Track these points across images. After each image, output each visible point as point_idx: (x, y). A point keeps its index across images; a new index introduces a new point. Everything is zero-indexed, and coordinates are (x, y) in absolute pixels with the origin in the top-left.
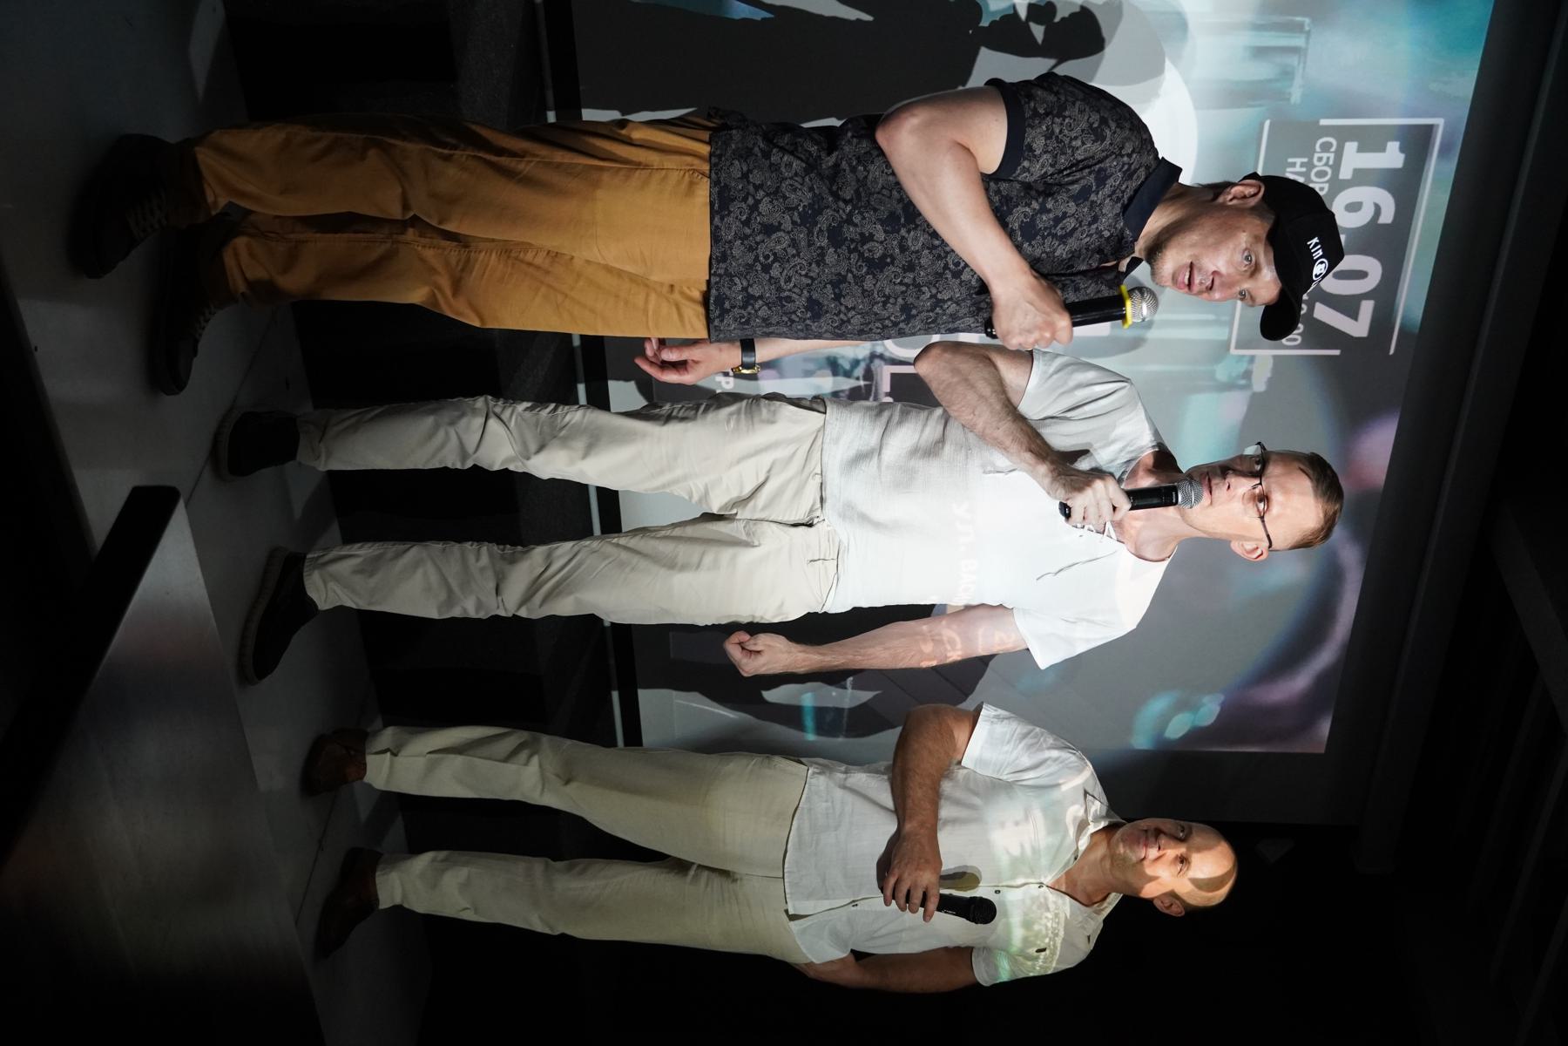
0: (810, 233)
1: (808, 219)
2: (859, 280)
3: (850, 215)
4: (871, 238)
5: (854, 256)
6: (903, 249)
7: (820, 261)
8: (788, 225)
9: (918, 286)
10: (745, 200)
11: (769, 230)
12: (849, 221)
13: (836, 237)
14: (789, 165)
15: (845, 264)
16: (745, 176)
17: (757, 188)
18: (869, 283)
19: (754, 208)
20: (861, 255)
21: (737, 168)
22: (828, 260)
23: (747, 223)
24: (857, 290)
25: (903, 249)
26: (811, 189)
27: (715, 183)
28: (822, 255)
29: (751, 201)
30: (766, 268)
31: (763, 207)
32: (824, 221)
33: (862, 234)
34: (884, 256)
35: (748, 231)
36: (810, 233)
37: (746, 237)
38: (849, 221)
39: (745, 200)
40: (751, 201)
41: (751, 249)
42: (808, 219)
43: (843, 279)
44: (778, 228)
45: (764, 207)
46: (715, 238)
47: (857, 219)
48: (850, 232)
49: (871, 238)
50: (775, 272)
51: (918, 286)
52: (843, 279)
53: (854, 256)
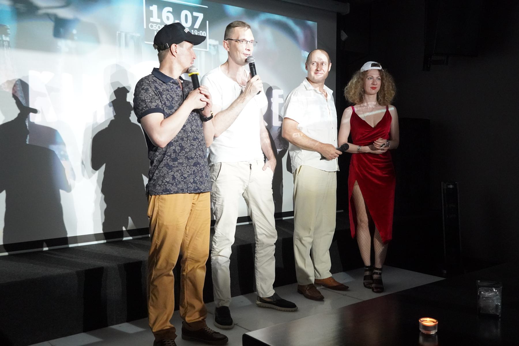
0: (174, 167)
1: (170, 168)
2: (186, 153)
3: (168, 156)
4: (174, 150)
5: (180, 154)
7: (182, 164)
10: (166, 185)
11: (174, 178)
12: (170, 156)
13: (175, 160)
14: (157, 174)
15: (182, 157)
16: (160, 186)
17: (163, 182)
18: (187, 150)
19: (168, 182)
20: (180, 152)
21: (158, 188)
22: (181, 162)
23: (172, 184)
24: (189, 153)
27: (162, 193)
28: (180, 163)
29: (166, 184)
31: (168, 180)
32: (171, 163)
33: (174, 152)
34: (179, 146)
35: (175, 184)
36: (174, 167)
37: (176, 184)
38: (170, 156)
39: (166, 185)
40: (166, 184)
41: (180, 183)
42: (170, 168)
43: (187, 157)
44: (173, 176)
45: (168, 180)
46: (177, 192)
47: (169, 154)
48: (173, 156)
49: (174, 150)
51: (188, 136)
53: (180, 154)
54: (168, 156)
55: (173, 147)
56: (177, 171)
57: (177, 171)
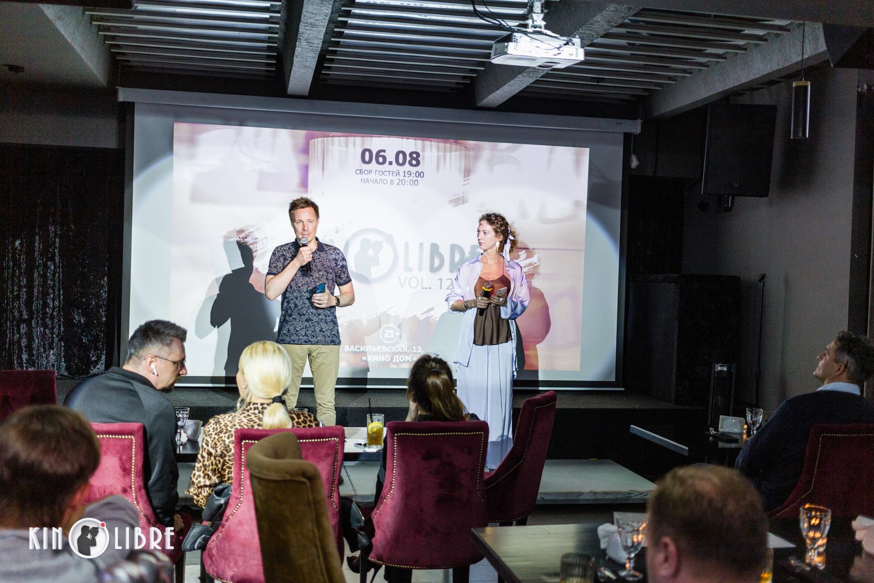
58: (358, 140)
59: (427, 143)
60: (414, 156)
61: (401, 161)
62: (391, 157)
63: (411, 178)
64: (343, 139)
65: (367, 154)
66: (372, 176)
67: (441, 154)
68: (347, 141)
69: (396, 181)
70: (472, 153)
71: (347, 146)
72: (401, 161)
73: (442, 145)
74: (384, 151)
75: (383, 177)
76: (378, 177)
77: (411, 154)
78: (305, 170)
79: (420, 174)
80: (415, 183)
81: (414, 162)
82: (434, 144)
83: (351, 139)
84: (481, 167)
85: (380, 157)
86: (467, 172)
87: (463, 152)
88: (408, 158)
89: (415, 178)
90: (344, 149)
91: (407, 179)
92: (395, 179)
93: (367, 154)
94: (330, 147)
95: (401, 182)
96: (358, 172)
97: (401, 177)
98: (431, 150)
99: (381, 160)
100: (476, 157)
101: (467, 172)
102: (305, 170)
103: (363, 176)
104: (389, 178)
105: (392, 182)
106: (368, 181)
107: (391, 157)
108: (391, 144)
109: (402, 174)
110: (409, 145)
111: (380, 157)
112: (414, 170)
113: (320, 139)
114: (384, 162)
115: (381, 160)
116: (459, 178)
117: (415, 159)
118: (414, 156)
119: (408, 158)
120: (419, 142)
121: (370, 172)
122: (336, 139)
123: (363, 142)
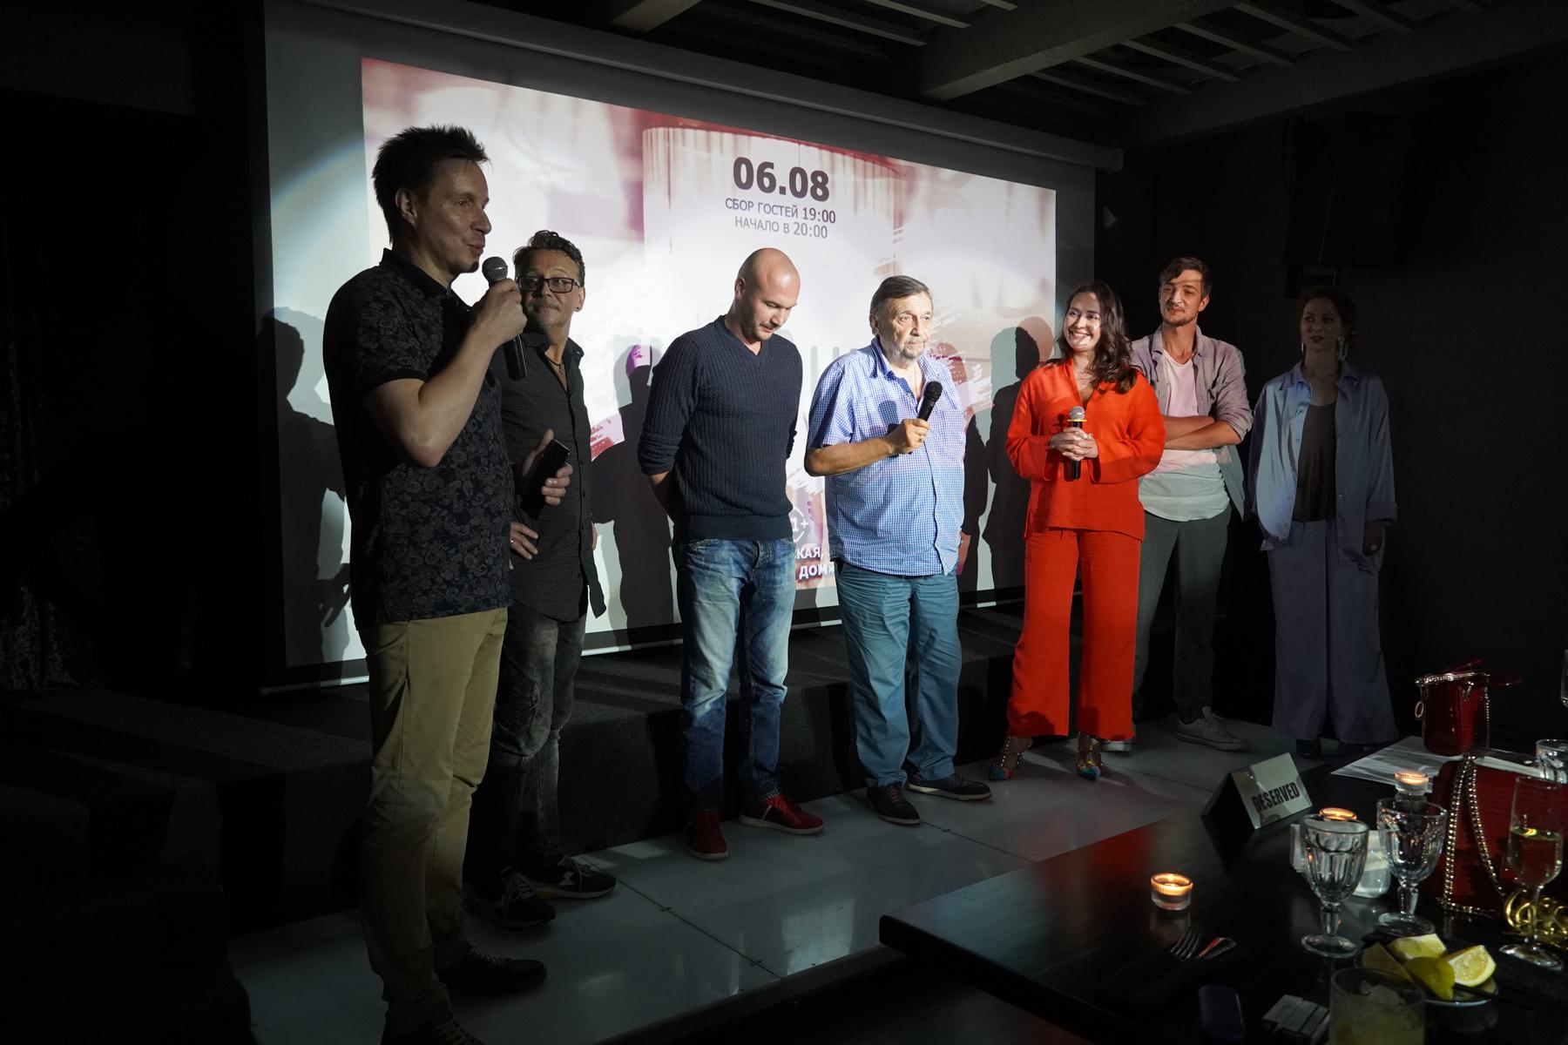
0: (462, 539)
2: (488, 498)
3: (444, 507)
4: (460, 491)
6: (466, 466)
7: (476, 528)
8: (458, 557)
9: (490, 453)
11: (463, 570)
18: (489, 491)
25: (466, 466)
26: (431, 542)
30: (489, 568)
36: (462, 539)
38: (449, 507)
43: (488, 510)
44: (461, 563)
45: (448, 576)
47: (447, 502)
49: (460, 491)
50: (490, 561)
52: (488, 510)
54: (444, 507)
55: (457, 484)
56: (470, 550)
57: (470, 550)
58: (728, 137)
59: (838, 157)
60: (820, 179)
61: (799, 188)
62: (783, 179)
63: (816, 222)
64: (701, 134)
65: (744, 167)
66: (753, 214)
67: (860, 179)
68: (708, 139)
69: (793, 228)
70: (904, 183)
71: (709, 150)
72: (799, 188)
73: (860, 162)
74: (771, 165)
75: (771, 218)
76: (764, 217)
77: (815, 174)
78: (637, 192)
79: (829, 216)
80: (822, 232)
81: (820, 192)
82: (849, 159)
83: (715, 135)
84: (917, 208)
85: (762, 176)
86: (899, 219)
87: (891, 180)
88: (810, 184)
89: (822, 224)
90: (704, 155)
91: (811, 224)
92: (791, 221)
93: (744, 167)
94: (680, 148)
95: (801, 230)
96: (730, 203)
97: (801, 221)
98: (843, 170)
99: (767, 182)
100: (910, 190)
101: (899, 219)
102: (637, 192)
103: (739, 213)
104: (781, 219)
105: (786, 227)
106: (746, 223)
107: (783, 179)
108: (784, 154)
109: (801, 213)
110: (811, 157)
111: (762, 176)
112: (820, 206)
113: (661, 130)
114: (770, 189)
115: (767, 182)
116: (887, 225)
117: (819, 185)
118: (820, 179)
119: (810, 184)
120: (826, 154)
121: (750, 205)
122: (689, 132)
123: (736, 142)
